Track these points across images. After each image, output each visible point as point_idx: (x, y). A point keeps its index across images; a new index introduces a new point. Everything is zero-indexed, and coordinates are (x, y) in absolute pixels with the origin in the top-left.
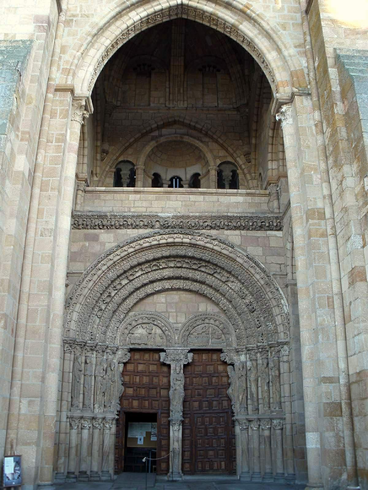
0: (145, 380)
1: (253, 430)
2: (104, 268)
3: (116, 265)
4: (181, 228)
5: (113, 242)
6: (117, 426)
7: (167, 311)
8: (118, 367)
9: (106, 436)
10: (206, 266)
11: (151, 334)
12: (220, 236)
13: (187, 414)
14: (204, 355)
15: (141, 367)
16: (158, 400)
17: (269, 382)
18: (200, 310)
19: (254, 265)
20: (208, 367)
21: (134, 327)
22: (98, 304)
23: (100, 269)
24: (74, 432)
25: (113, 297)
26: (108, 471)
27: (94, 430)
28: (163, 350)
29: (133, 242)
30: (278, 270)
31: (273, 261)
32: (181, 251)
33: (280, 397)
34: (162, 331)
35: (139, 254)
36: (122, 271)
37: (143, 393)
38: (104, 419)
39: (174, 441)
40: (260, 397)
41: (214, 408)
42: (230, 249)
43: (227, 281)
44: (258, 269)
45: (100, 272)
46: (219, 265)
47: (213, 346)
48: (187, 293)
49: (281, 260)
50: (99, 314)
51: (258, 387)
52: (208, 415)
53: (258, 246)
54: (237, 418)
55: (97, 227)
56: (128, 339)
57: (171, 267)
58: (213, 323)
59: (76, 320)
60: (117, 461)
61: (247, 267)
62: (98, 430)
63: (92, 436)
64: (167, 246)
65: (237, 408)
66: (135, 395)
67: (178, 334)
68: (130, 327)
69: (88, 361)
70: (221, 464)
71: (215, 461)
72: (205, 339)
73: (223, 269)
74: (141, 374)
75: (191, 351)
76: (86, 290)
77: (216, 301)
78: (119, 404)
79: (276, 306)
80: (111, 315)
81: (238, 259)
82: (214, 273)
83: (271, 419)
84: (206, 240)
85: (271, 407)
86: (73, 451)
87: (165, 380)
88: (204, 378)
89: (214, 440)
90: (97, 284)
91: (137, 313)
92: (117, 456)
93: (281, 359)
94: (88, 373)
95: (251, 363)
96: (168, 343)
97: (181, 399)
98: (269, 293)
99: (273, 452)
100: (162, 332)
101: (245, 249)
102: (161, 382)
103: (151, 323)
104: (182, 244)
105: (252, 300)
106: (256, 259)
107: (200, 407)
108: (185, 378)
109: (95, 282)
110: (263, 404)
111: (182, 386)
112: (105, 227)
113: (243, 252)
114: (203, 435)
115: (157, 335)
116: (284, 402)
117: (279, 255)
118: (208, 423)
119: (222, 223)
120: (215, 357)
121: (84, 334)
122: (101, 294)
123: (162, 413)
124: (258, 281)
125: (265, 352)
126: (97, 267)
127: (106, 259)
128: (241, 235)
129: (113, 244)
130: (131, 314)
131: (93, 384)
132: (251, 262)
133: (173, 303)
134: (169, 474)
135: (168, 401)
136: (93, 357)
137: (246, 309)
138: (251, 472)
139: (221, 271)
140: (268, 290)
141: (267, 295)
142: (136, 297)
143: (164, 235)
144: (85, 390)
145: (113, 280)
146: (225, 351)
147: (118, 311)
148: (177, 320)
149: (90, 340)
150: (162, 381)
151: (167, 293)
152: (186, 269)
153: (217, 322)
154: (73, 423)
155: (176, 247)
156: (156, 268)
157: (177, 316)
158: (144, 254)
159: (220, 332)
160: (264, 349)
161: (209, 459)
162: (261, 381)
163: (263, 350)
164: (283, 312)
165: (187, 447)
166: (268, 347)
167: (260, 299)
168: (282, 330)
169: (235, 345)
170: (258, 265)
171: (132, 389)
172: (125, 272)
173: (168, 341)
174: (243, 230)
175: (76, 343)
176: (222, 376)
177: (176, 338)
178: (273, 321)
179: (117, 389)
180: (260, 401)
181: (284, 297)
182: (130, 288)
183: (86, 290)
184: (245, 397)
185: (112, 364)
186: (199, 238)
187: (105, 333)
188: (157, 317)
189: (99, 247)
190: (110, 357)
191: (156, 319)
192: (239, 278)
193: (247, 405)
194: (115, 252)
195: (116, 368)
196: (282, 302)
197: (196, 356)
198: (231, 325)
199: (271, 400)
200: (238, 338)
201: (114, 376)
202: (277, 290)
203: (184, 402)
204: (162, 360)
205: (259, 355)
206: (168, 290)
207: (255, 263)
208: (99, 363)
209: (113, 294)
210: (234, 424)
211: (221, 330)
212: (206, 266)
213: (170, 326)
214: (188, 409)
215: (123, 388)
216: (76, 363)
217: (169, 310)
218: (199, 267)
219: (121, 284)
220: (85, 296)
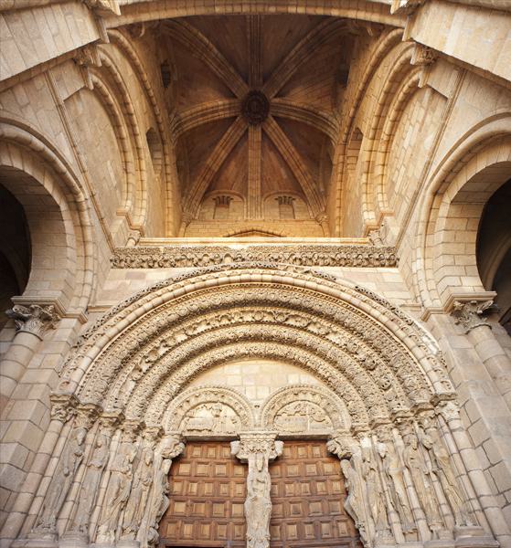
0: (208, 489)
14: (299, 449)
15: (201, 469)
19: (367, 298)
20: (308, 466)
21: (193, 408)
23: (140, 306)
25: (162, 357)
34: (235, 411)
42: (330, 283)
43: (327, 334)
50: (136, 375)
56: (183, 423)
57: (248, 323)
64: (241, 287)
72: (300, 422)
73: (319, 314)
77: (313, 366)
81: (344, 295)
82: (309, 324)
84: (295, 275)
87: (240, 489)
88: (303, 485)
100: (234, 414)
102: (232, 492)
104: (261, 284)
119: (316, 256)
120: (317, 450)
124: (377, 320)
130: (190, 388)
135: (243, 522)
137: (362, 369)
147: (170, 381)
150: (235, 491)
153: (317, 396)
156: (227, 322)
157: (257, 390)
159: (323, 411)
166: (412, 415)
172: (181, 320)
173: (245, 424)
187: (144, 407)
190: (148, 444)
192: (347, 321)
195: (156, 466)
197: (288, 451)
209: (162, 351)
211: (324, 409)
220: (110, 340)
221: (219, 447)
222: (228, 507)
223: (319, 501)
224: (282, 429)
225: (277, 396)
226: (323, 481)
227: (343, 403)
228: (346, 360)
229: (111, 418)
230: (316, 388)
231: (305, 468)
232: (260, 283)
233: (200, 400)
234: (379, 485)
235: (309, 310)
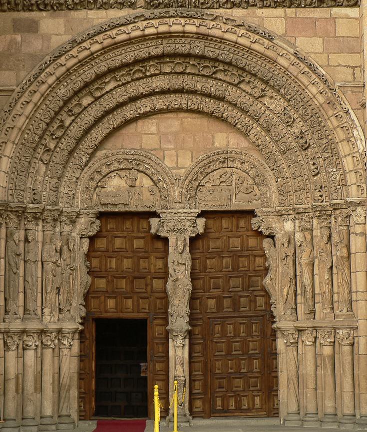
0: (127, 263)
1: (306, 345)
2: (51, 80)
3: (71, 73)
4: (181, 6)
5: (65, 33)
6: (80, 342)
7: (160, 149)
8: (81, 246)
9: (64, 359)
10: (225, 71)
11: (134, 186)
12: (250, 19)
13: (197, 319)
15: (118, 243)
16: (147, 298)
17: (331, 268)
18: (217, 144)
19: (307, 69)
20: (231, 240)
22: (43, 142)
23: (43, 83)
24: (11, 355)
25: (68, 128)
26: (69, 416)
27: (44, 350)
28: (154, 214)
29: (99, 33)
30: (350, 78)
31: (340, 62)
32: (183, 48)
33: (350, 292)
34: (154, 182)
35: (110, 53)
36: (81, 84)
38: (60, 331)
39: (176, 364)
40: (317, 291)
41: (242, 309)
42: (266, 41)
43: (262, 97)
44: (314, 76)
45: (44, 87)
46: (247, 69)
47: (238, 206)
48: (194, 115)
49: (353, 60)
50: (46, 157)
51: (313, 275)
52: (232, 321)
53: (316, 35)
54: (278, 326)
55: (35, 8)
56: (95, 196)
58: (239, 166)
59: (8, 170)
60: (82, 398)
61: (295, 74)
62: (51, 350)
63: (41, 360)
64: (158, 38)
65: (279, 309)
67: (180, 186)
68: (98, 177)
69: (30, 238)
70: (254, 401)
71: (246, 396)
72: (225, 194)
73: (255, 75)
74: (119, 254)
75: (202, 214)
76: (23, 119)
77: (244, 129)
78: (84, 306)
79: (343, 140)
80: (65, 158)
81: (281, 60)
82: (240, 82)
83: (335, 329)
85: (335, 308)
86: (12, 386)
87: (160, 264)
88: (224, 260)
89: (242, 362)
90: (40, 108)
91: (109, 153)
92: (83, 390)
93: (352, 229)
94: (31, 257)
95: (302, 236)
96: (164, 202)
98: (333, 119)
99: (338, 382)
100: (152, 184)
101: (293, 41)
102: (152, 267)
103: (133, 168)
104: (184, 34)
105: (304, 129)
106: (312, 59)
107: (220, 306)
108: (193, 259)
109: (36, 105)
110: (323, 303)
111: (188, 275)
112: (49, 8)
113: (289, 49)
114: (223, 353)
115: (144, 188)
116: (357, 301)
117: (352, 51)
118: (232, 335)
120: (242, 223)
121: (22, 192)
122: (48, 124)
123: (156, 319)
124: (314, 97)
125: (325, 217)
126: (39, 78)
127: (53, 65)
128: (286, 17)
129: (64, 37)
130: (100, 154)
131: (40, 275)
132: (302, 66)
133: (171, 133)
134: (168, 418)
135: (165, 298)
136: (38, 231)
138: (302, 413)
139: (252, 80)
140: (331, 113)
141: (328, 121)
142: (107, 125)
143: (151, 19)
144: (27, 287)
145: (65, 98)
146: (259, 214)
147: (77, 151)
148: (177, 163)
149: (33, 203)
150: (155, 266)
151: (160, 116)
152: (191, 76)
153: (246, 164)
154: (9, 341)
155: (173, 39)
156: (141, 75)
157: (177, 156)
158: (119, 53)
159: (251, 181)
160: (323, 212)
161: (234, 392)
162: (319, 265)
163: (323, 214)
164: (356, 150)
165: (197, 373)
167: (317, 128)
168: (354, 181)
169: (275, 204)
170: (314, 70)
171: (104, 280)
172: (87, 85)
174: (289, 7)
175: (9, 209)
176: (255, 256)
178: (338, 164)
179: (81, 280)
180: (318, 299)
181: (358, 125)
182: (96, 111)
183: (23, 119)
184: (292, 292)
185: (70, 240)
186: (212, 23)
187: (56, 189)
188: (143, 158)
189: (41, 41)
190: (67, 228)
191: (142, 162)
192: (282, 91)
193: (296, 305)
194: (69, 51)
196: (355, 133)
197: (211, 222)
198: (268, 169)
199: (336, 297)
200: (281, 191)
201: (74, 260)
202: (347, 112)
203: (192, 299)
204: (153, 231)
205: (315, 221)
206: (161, 111)
207: (310, 66)
208: (48, 241)
209: (67, 123)
210: (275, 335)
212: (225, 71)
213: (166, 174)
214: (198, 311)
215: (89, 279)
216: (11, 243)
217: (164, 146)
218: (214, 73)
219: (81, 105)
220: (20, 129)
221: (136, 219)
222: (149, 281)
223: (240, 276)
224: (204, 203)
225: (200, 165)
226: (246, 256)
227: (273, 177)
228: (281, 129)
229: (35, 213)
230: (246, 154)
231: (229, 242)
232: (181, 35)
233: (112, 168)
234: (291, 272)
235: (243, 69)
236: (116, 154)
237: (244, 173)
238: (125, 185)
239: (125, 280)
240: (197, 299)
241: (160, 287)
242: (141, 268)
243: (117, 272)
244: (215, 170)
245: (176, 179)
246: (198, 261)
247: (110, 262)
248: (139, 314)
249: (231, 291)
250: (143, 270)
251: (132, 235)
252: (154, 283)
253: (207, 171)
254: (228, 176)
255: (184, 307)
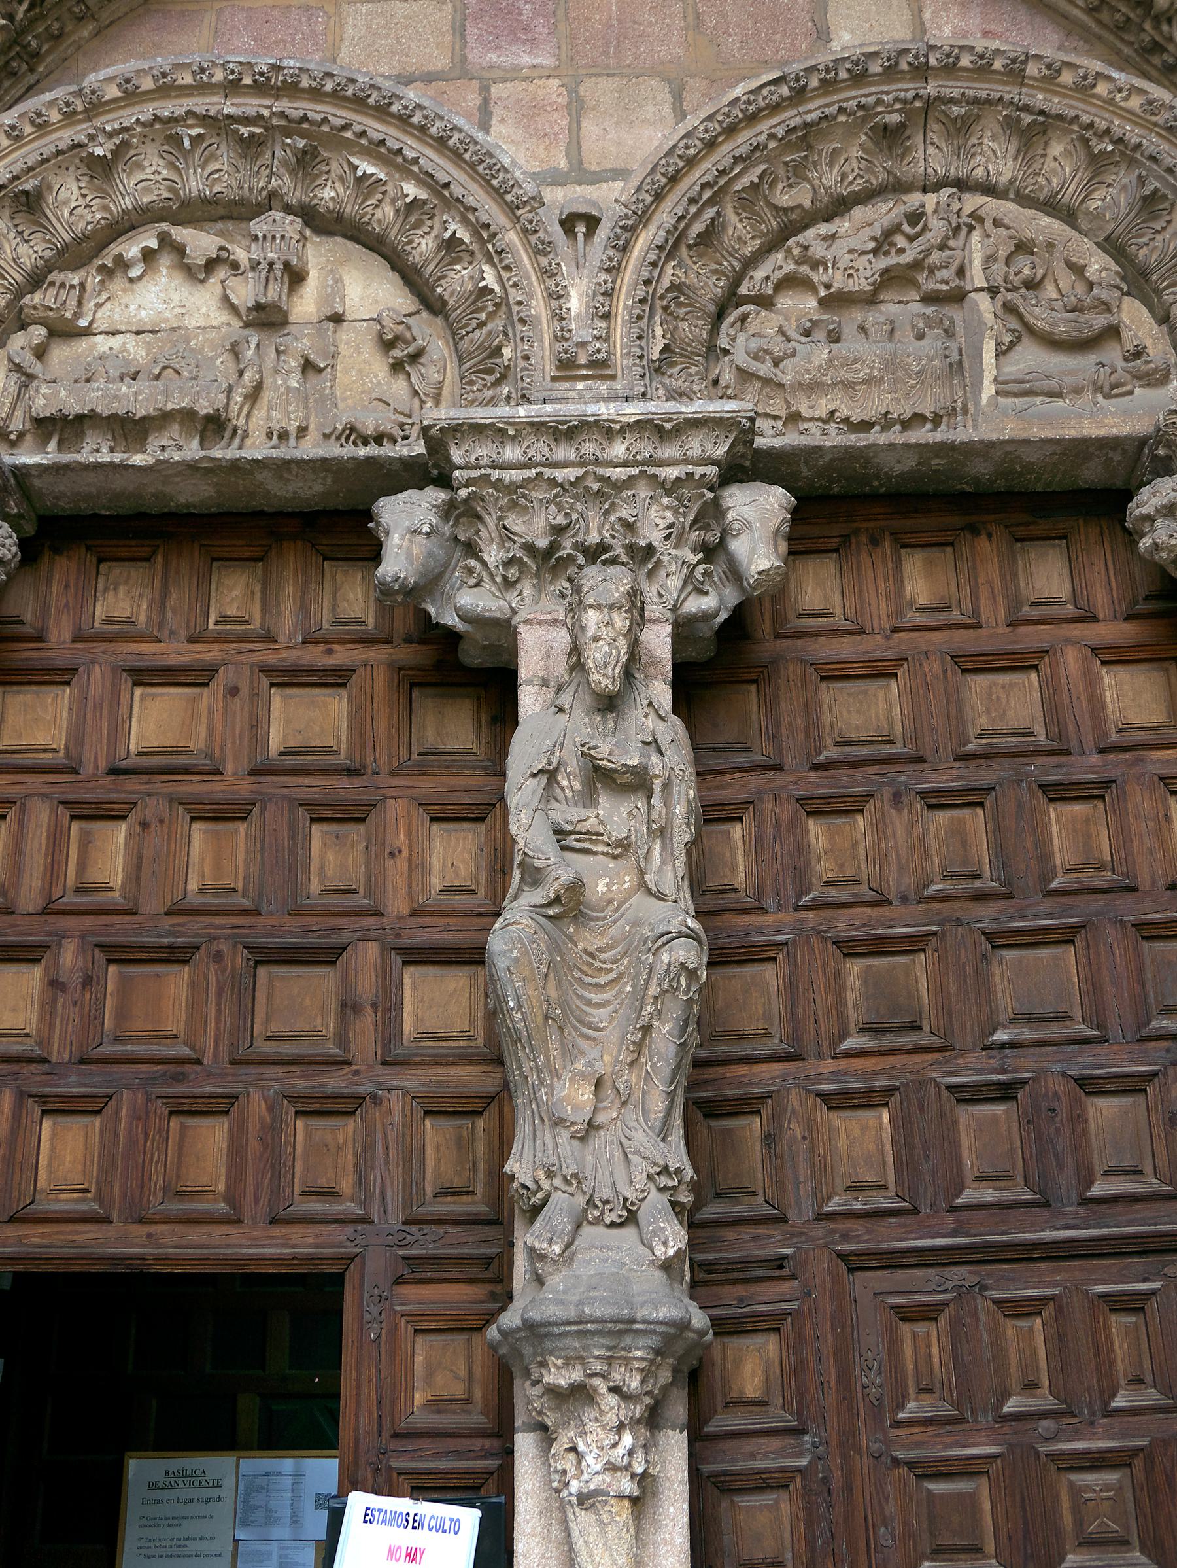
20: (980, 681)
37: (174, 1018)
58: (1004, 169)
66: (58, 1053)
97: (665, 1034)
103: (272, 200)
115: (344, 335)
150: (418, 867)
153: (1056, 149)
157: (577, 108)
159: (1098, 265)
177: (575, 304)
188: (339, 115)
213: (499, 194)
214: (758, 1206)
236: (147, 84)
237: (1045, 220)
238: (220, 317)
239: (182, 975)
240: (747, 1106)
241: (461, 1024)
242: (315, 886)
243: (132, 912)
244: (840, 206)
245: (568, 223)
246: (737, 830)
247: (86, 842)
248: (279, 1231)
249: (1003, 1046)
250: (325, 900)
251: (265, 656)
252: (408, 993)
253: (784, 199)
254: (937, 228)
255: (642, 1138)
